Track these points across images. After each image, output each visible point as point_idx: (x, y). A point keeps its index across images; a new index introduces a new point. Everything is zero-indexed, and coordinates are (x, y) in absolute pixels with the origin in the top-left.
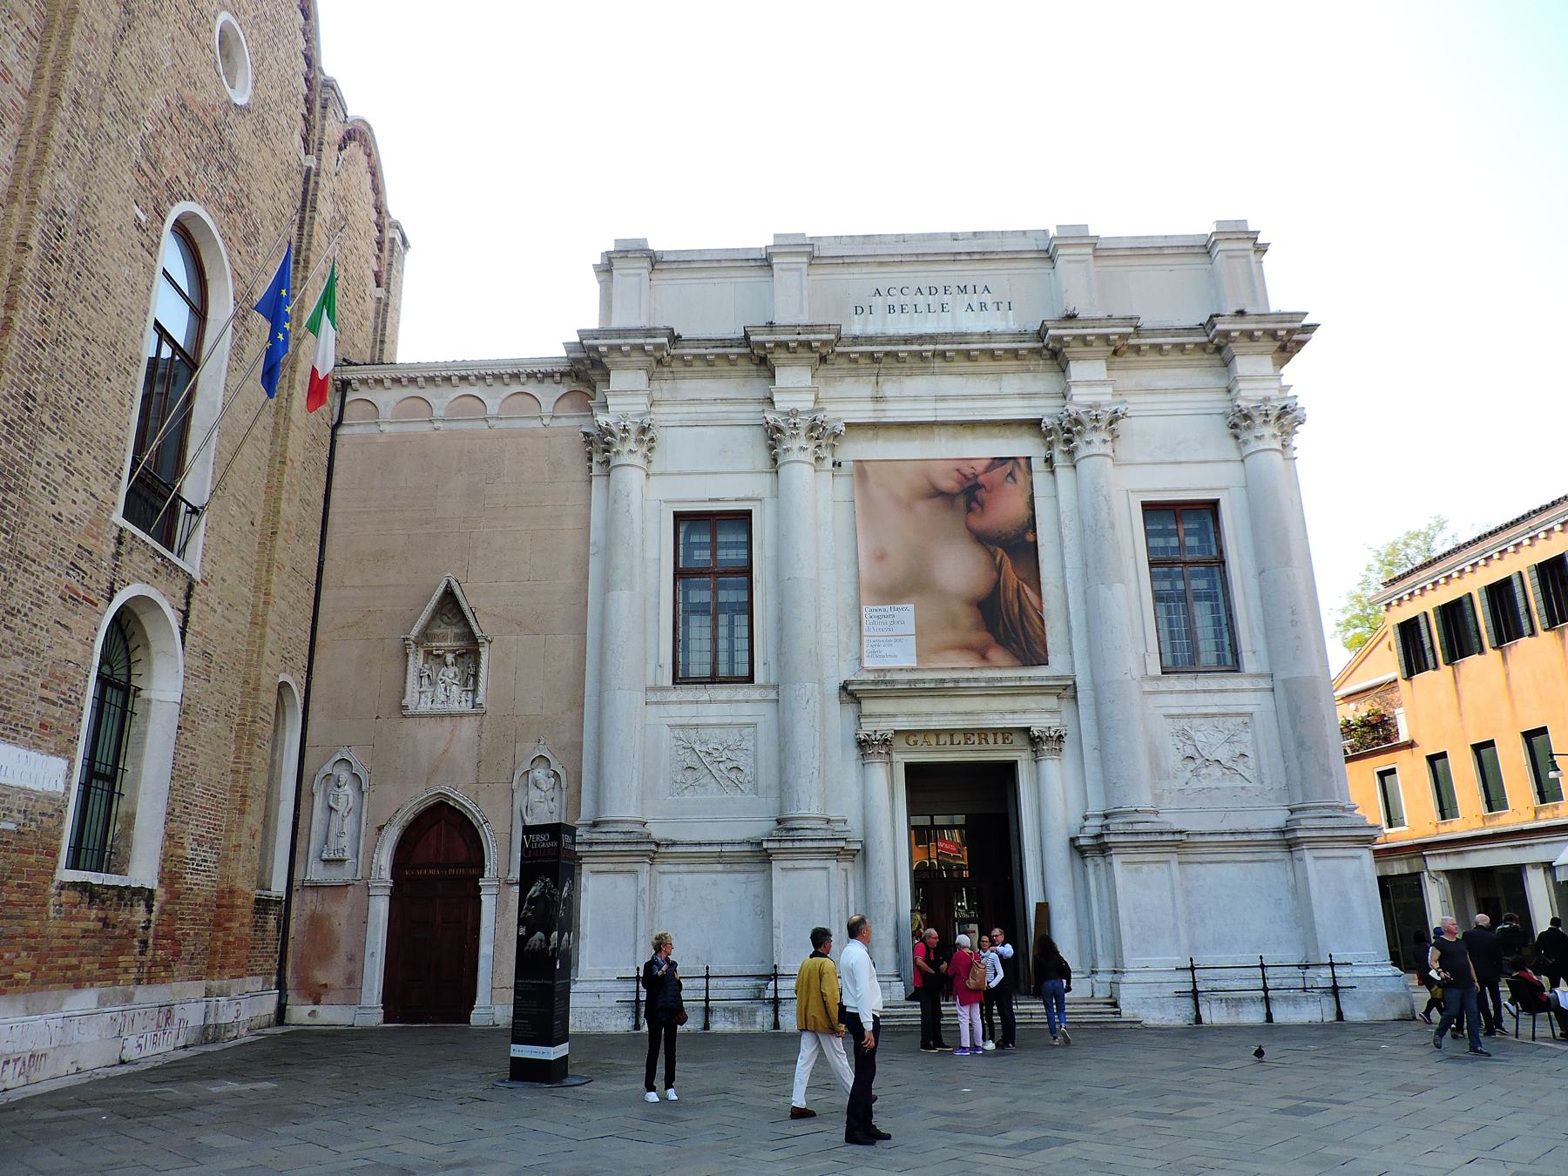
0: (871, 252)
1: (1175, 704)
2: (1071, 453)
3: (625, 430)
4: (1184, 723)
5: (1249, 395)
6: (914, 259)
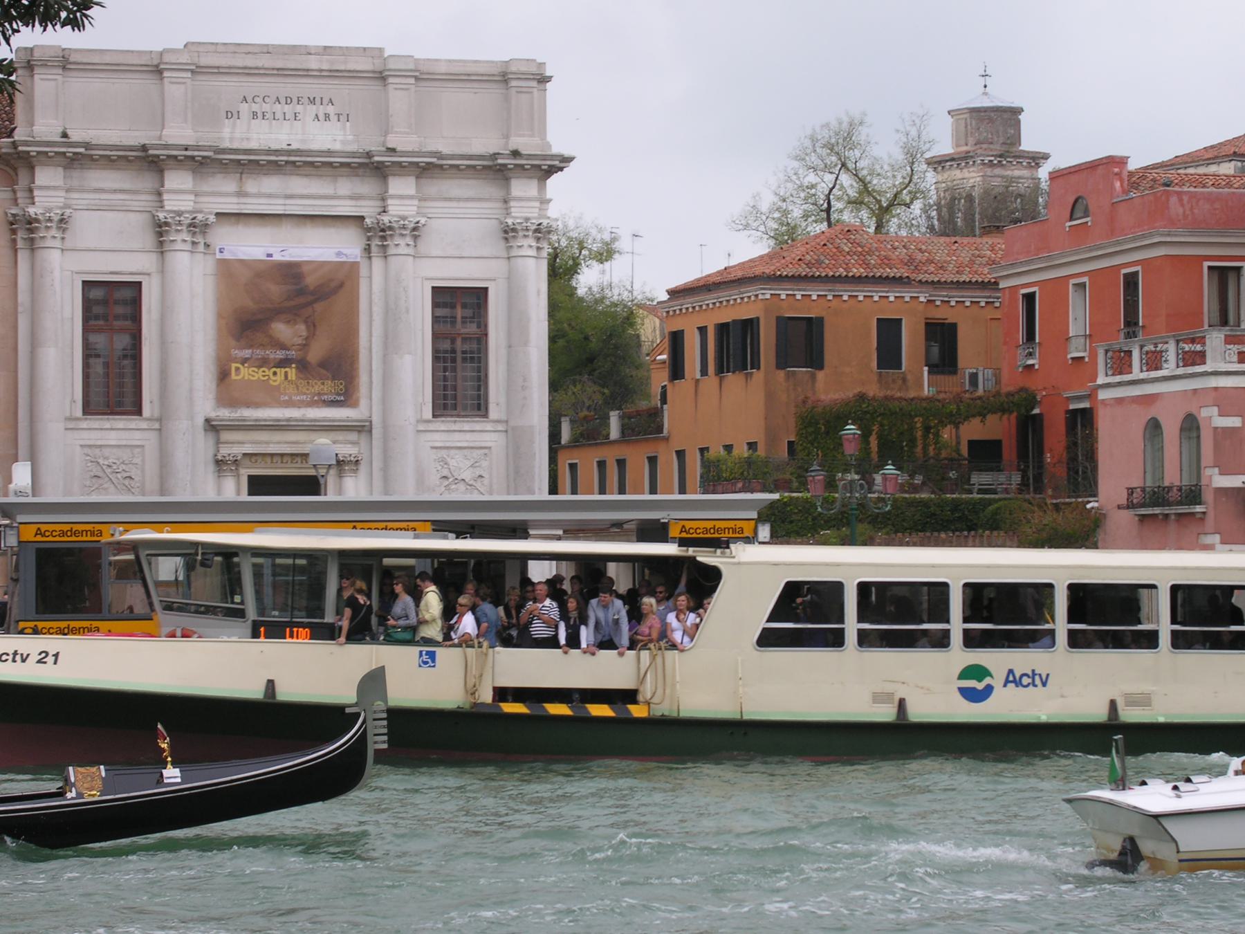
0: (240, 65)
1: (439, 439)
2: (384, 247)
3: (50, 220)
4: (444, 453)
5: (519, 212)
6: (275, 72)
